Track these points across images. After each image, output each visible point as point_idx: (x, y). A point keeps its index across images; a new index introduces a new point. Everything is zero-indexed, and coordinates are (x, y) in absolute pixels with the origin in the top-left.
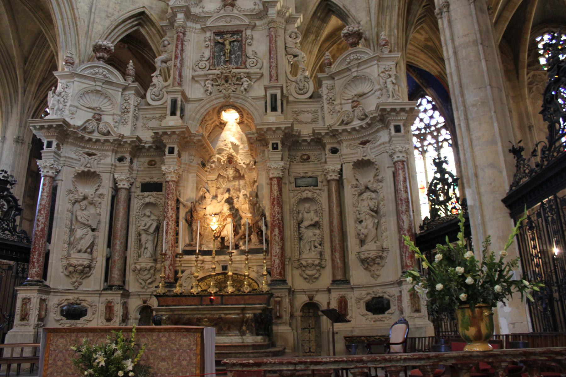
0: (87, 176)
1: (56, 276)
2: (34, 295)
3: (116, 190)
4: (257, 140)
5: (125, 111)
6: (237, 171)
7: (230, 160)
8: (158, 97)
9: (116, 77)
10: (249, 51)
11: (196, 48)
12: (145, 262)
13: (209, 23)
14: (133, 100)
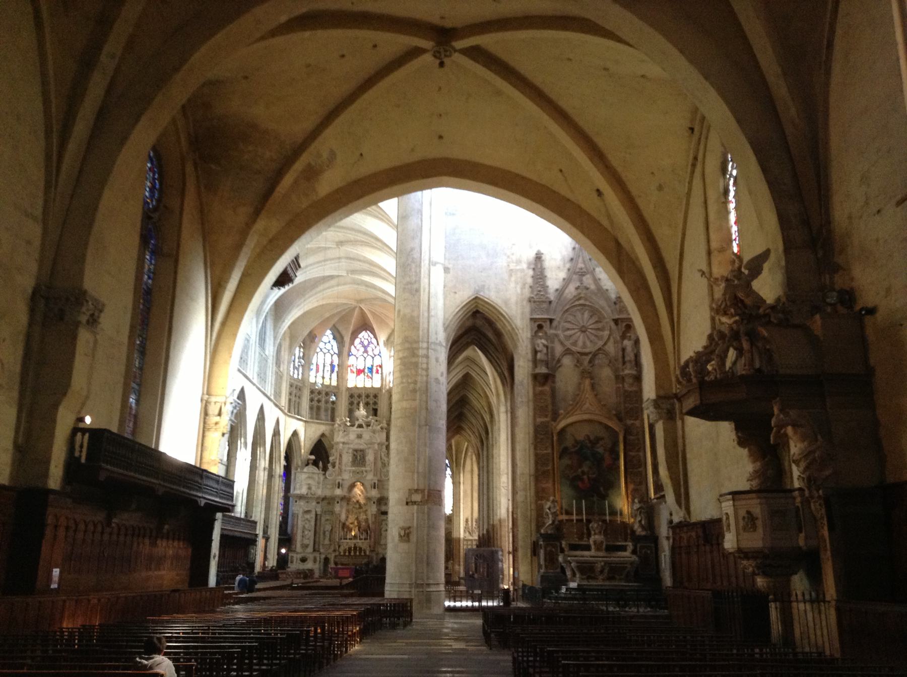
0: (308, 512)
1: (299, 548)
2: (295, 555)
3: (316, 515)
4: (368, 499)
5: (319, 483)
6: (360, 505)
7: (358, 501)
8: (330, 475)
9: (315, 470)
10: (367, 458)
11: (347, 458)
12: (327, 542)
13: (352, 446)
14: (322, 478)
